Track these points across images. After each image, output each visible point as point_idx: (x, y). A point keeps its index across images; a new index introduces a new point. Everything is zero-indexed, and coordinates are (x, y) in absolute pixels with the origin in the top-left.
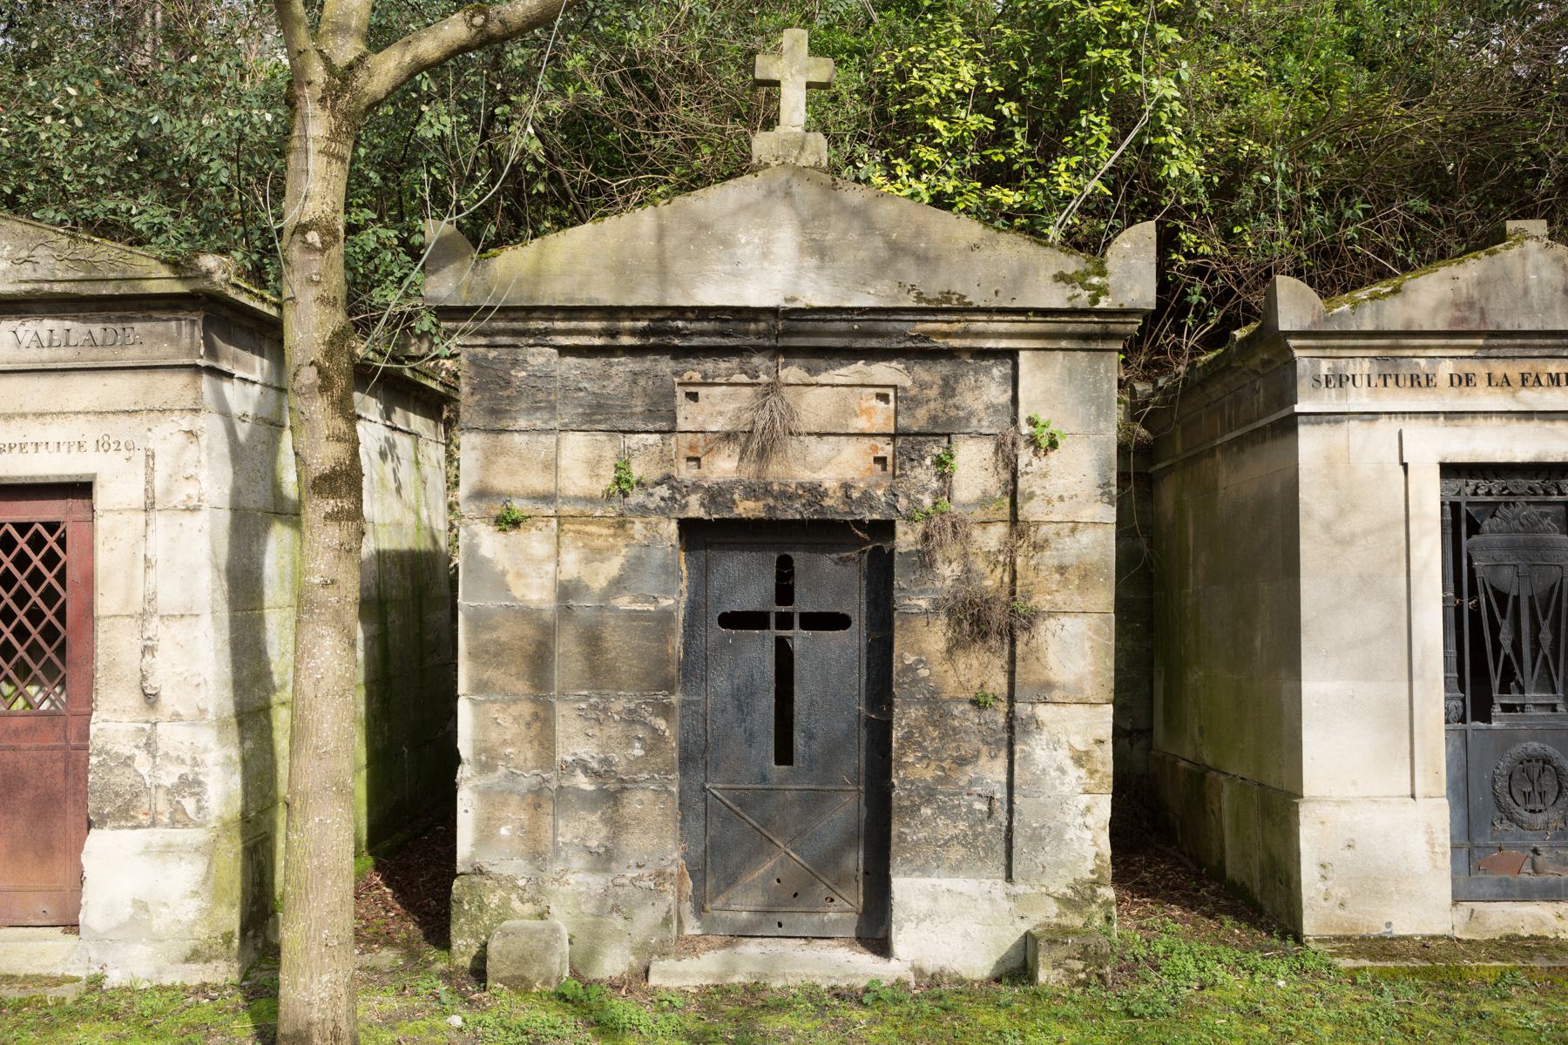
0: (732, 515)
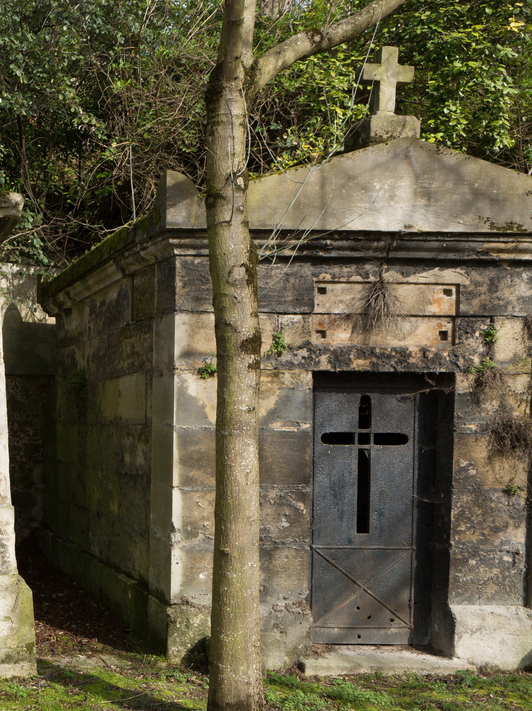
0: (349, 369)
